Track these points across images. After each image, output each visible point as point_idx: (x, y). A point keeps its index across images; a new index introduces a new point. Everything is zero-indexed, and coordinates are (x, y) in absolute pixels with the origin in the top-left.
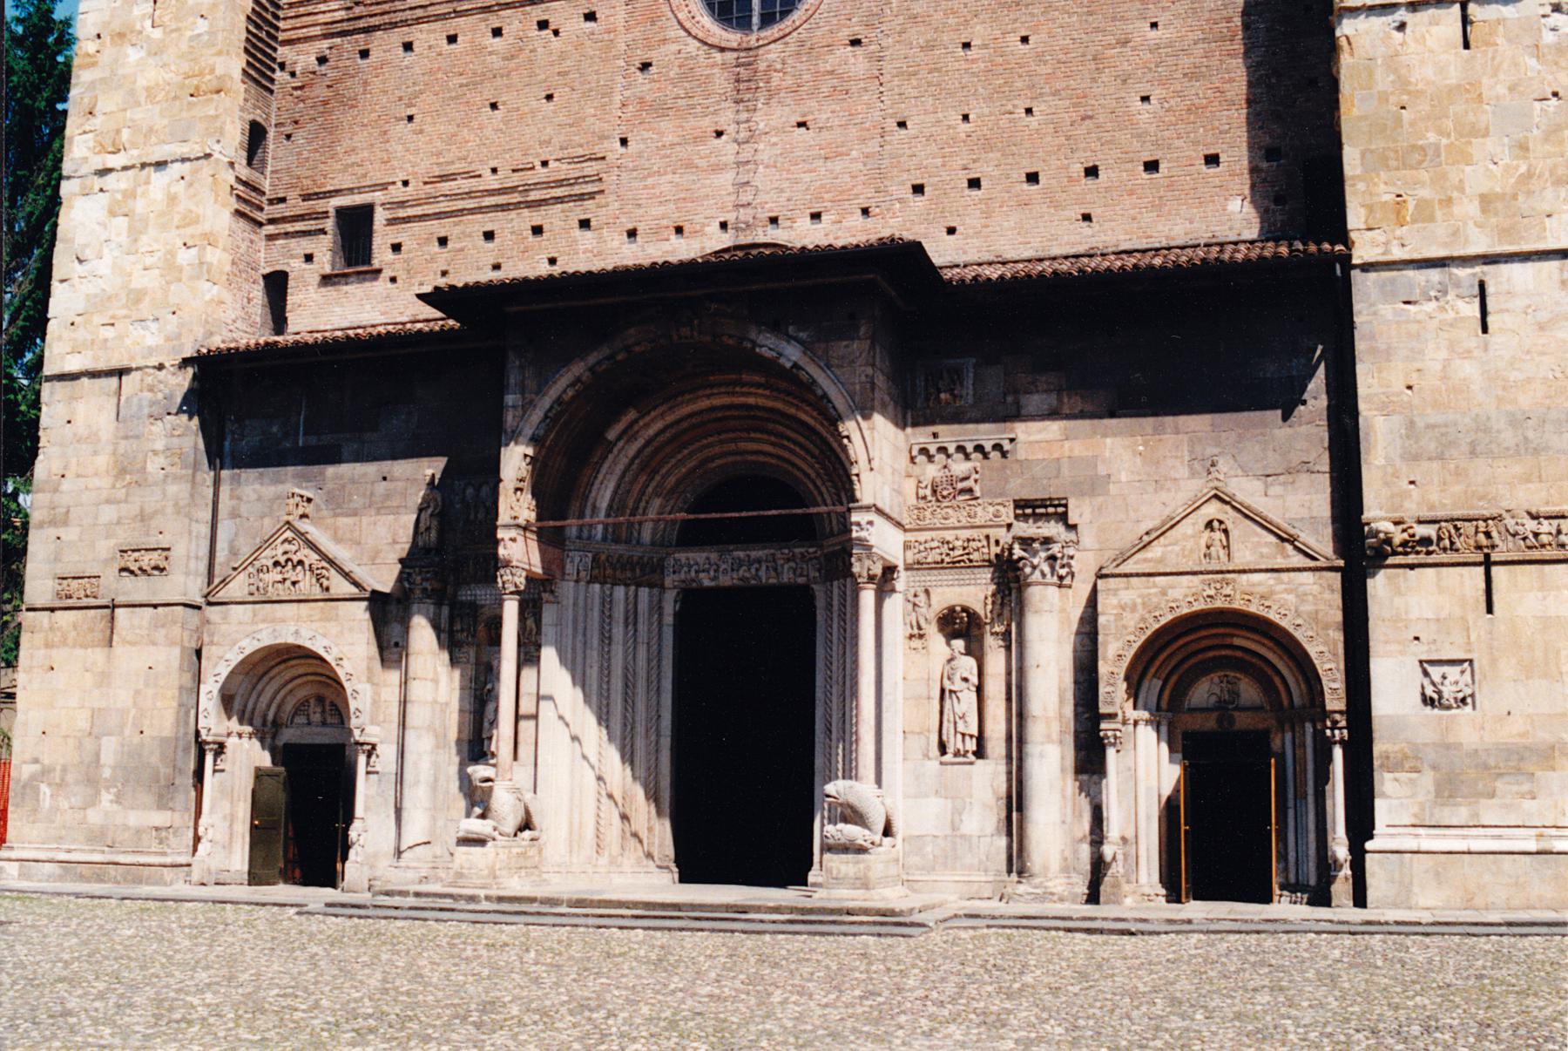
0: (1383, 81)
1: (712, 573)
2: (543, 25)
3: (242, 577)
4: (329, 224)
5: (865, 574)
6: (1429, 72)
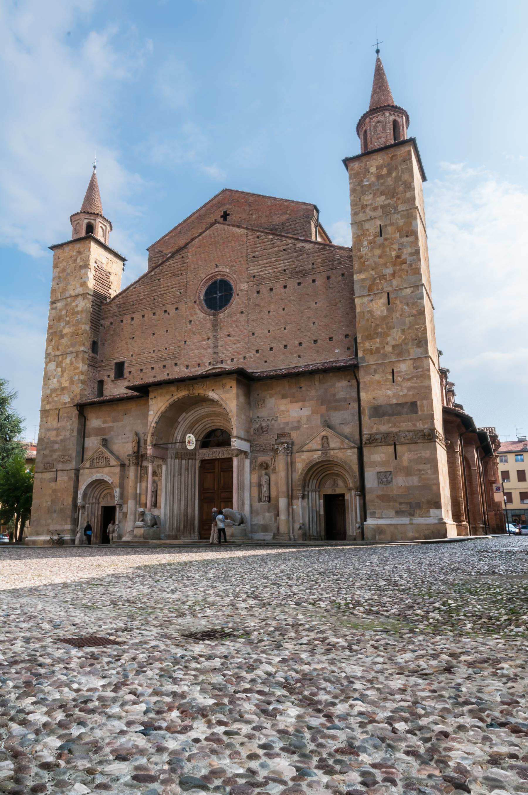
0: (367, 316)
2: (165, 311)
3: (89, 462)
4: (114, 367)
6: (379, 313)
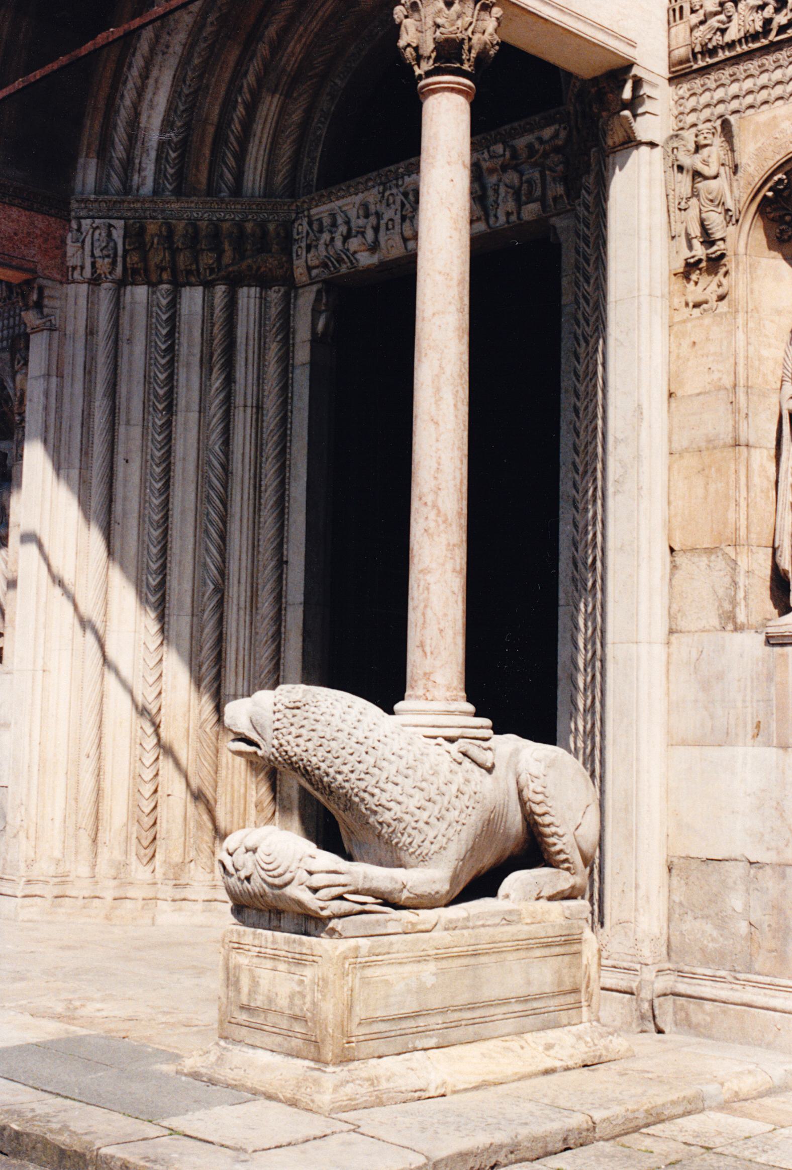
1: (370, 234)
5: (428, 47)
